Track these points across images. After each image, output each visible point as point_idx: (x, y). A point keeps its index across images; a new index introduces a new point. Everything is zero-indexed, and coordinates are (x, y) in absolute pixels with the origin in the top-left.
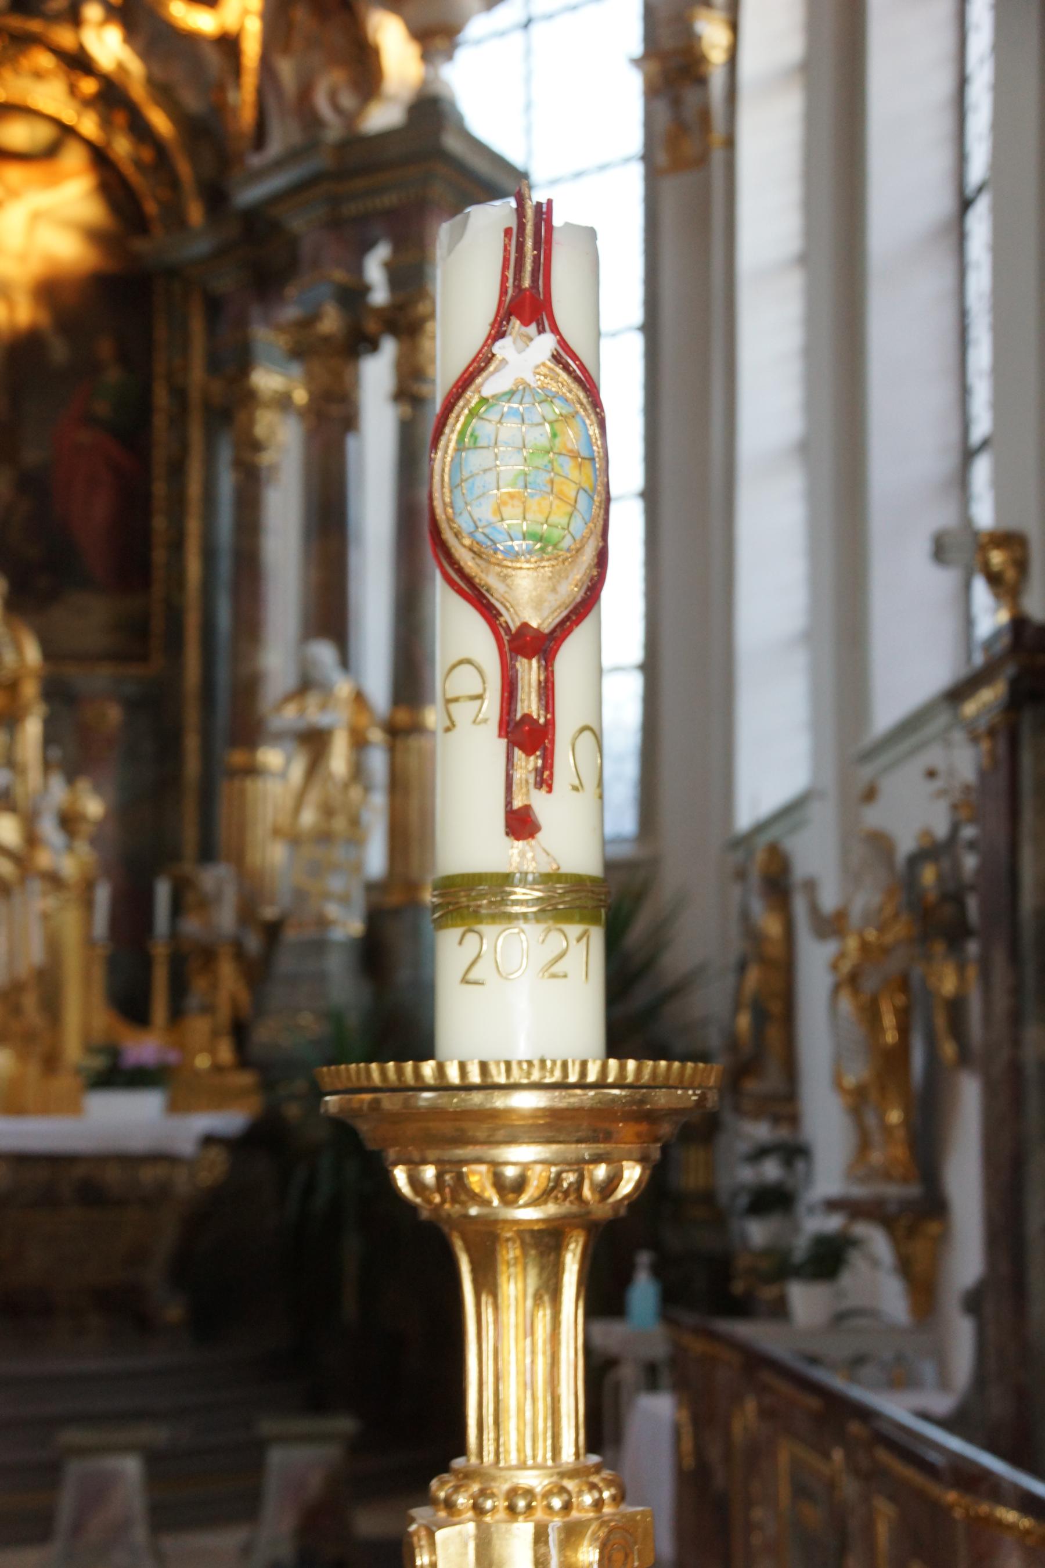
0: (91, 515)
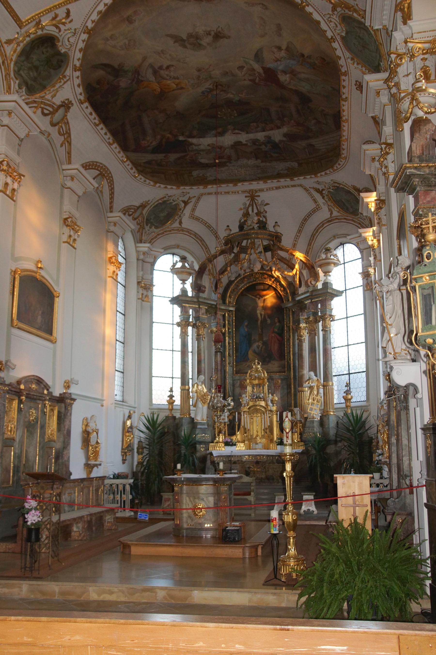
0: (275, 347)
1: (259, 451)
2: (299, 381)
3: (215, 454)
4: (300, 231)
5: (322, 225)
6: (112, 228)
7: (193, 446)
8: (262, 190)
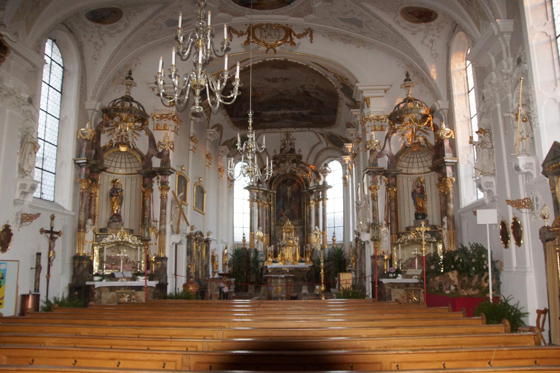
1: (290, 265)
2: (309, 231)
3: (269, 267)
4: (310, 152)
6: (221, 154)
7: (256, 262)
8: (292, 132)
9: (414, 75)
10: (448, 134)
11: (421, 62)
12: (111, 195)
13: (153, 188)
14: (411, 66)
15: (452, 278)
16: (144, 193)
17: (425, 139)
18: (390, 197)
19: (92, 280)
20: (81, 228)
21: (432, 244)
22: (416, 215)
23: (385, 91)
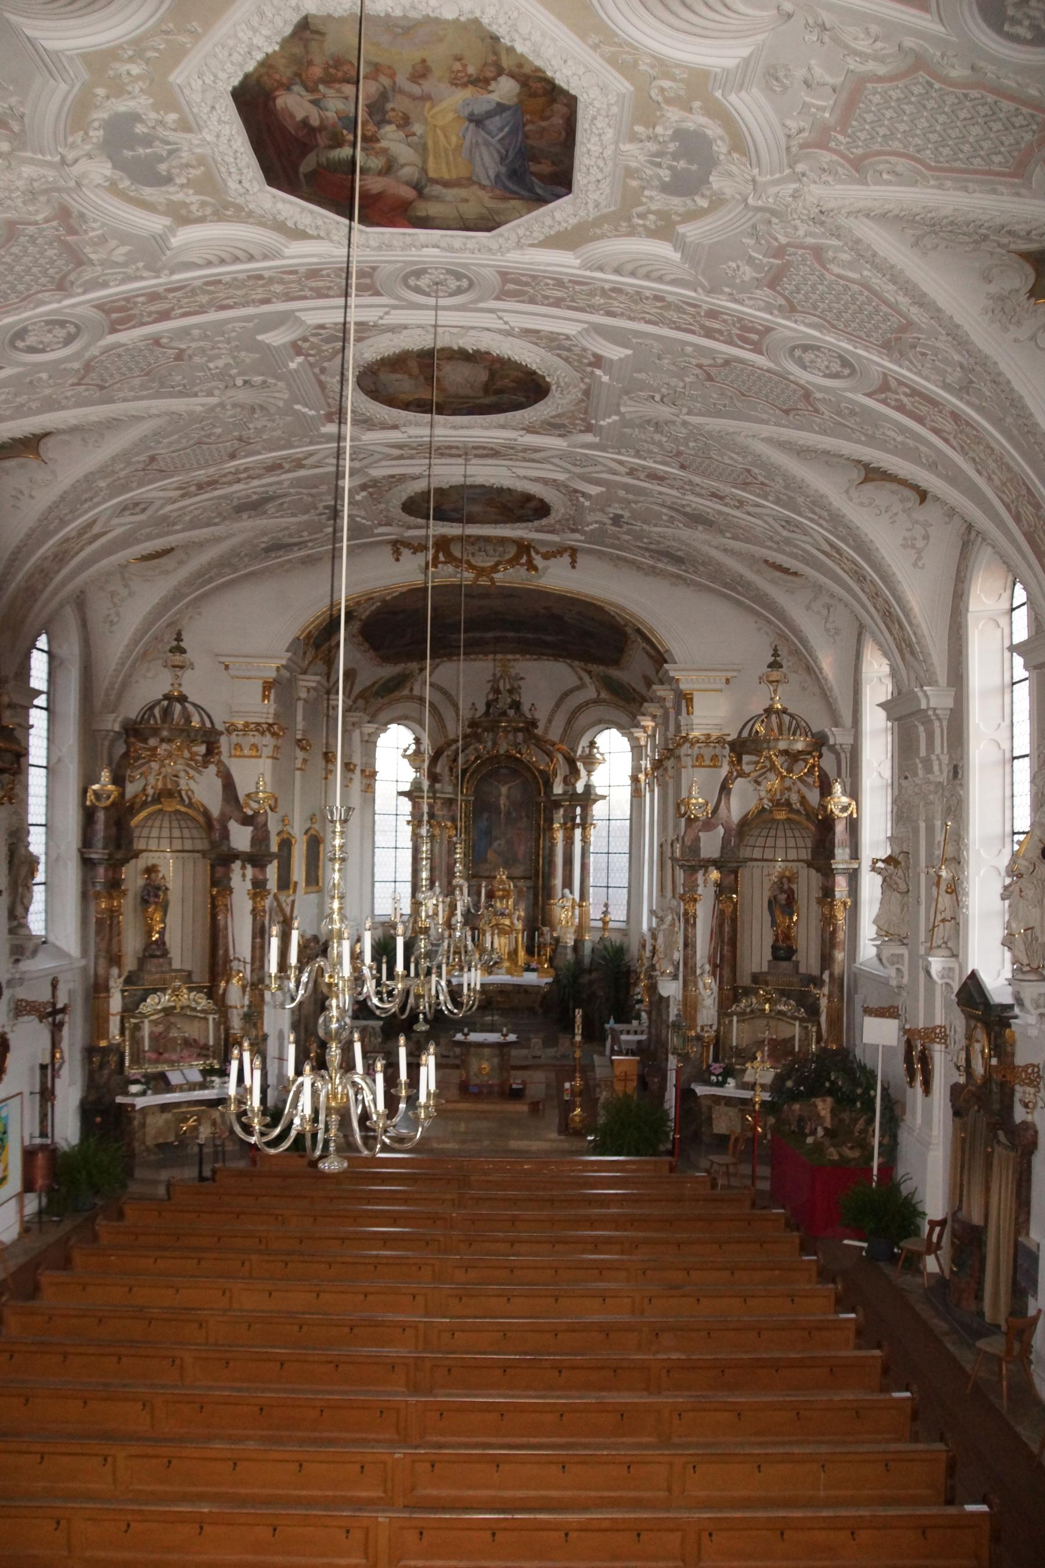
2: (548, 892)
4: (558, 705)
5: (586, 704)
9: (787, 656)
10: (844, 809)
11: (804, 641)
12: (145, 902)
13: (233, 884)
14: (782, 636)
15: (823, 1113)
16: (213, 898)
17: (803, 800)
18: (722, 912)
19: (126, 1093)
20: (97, 989)
21: (797, 1023)
22: (775, 948)
23: (728, 681)
